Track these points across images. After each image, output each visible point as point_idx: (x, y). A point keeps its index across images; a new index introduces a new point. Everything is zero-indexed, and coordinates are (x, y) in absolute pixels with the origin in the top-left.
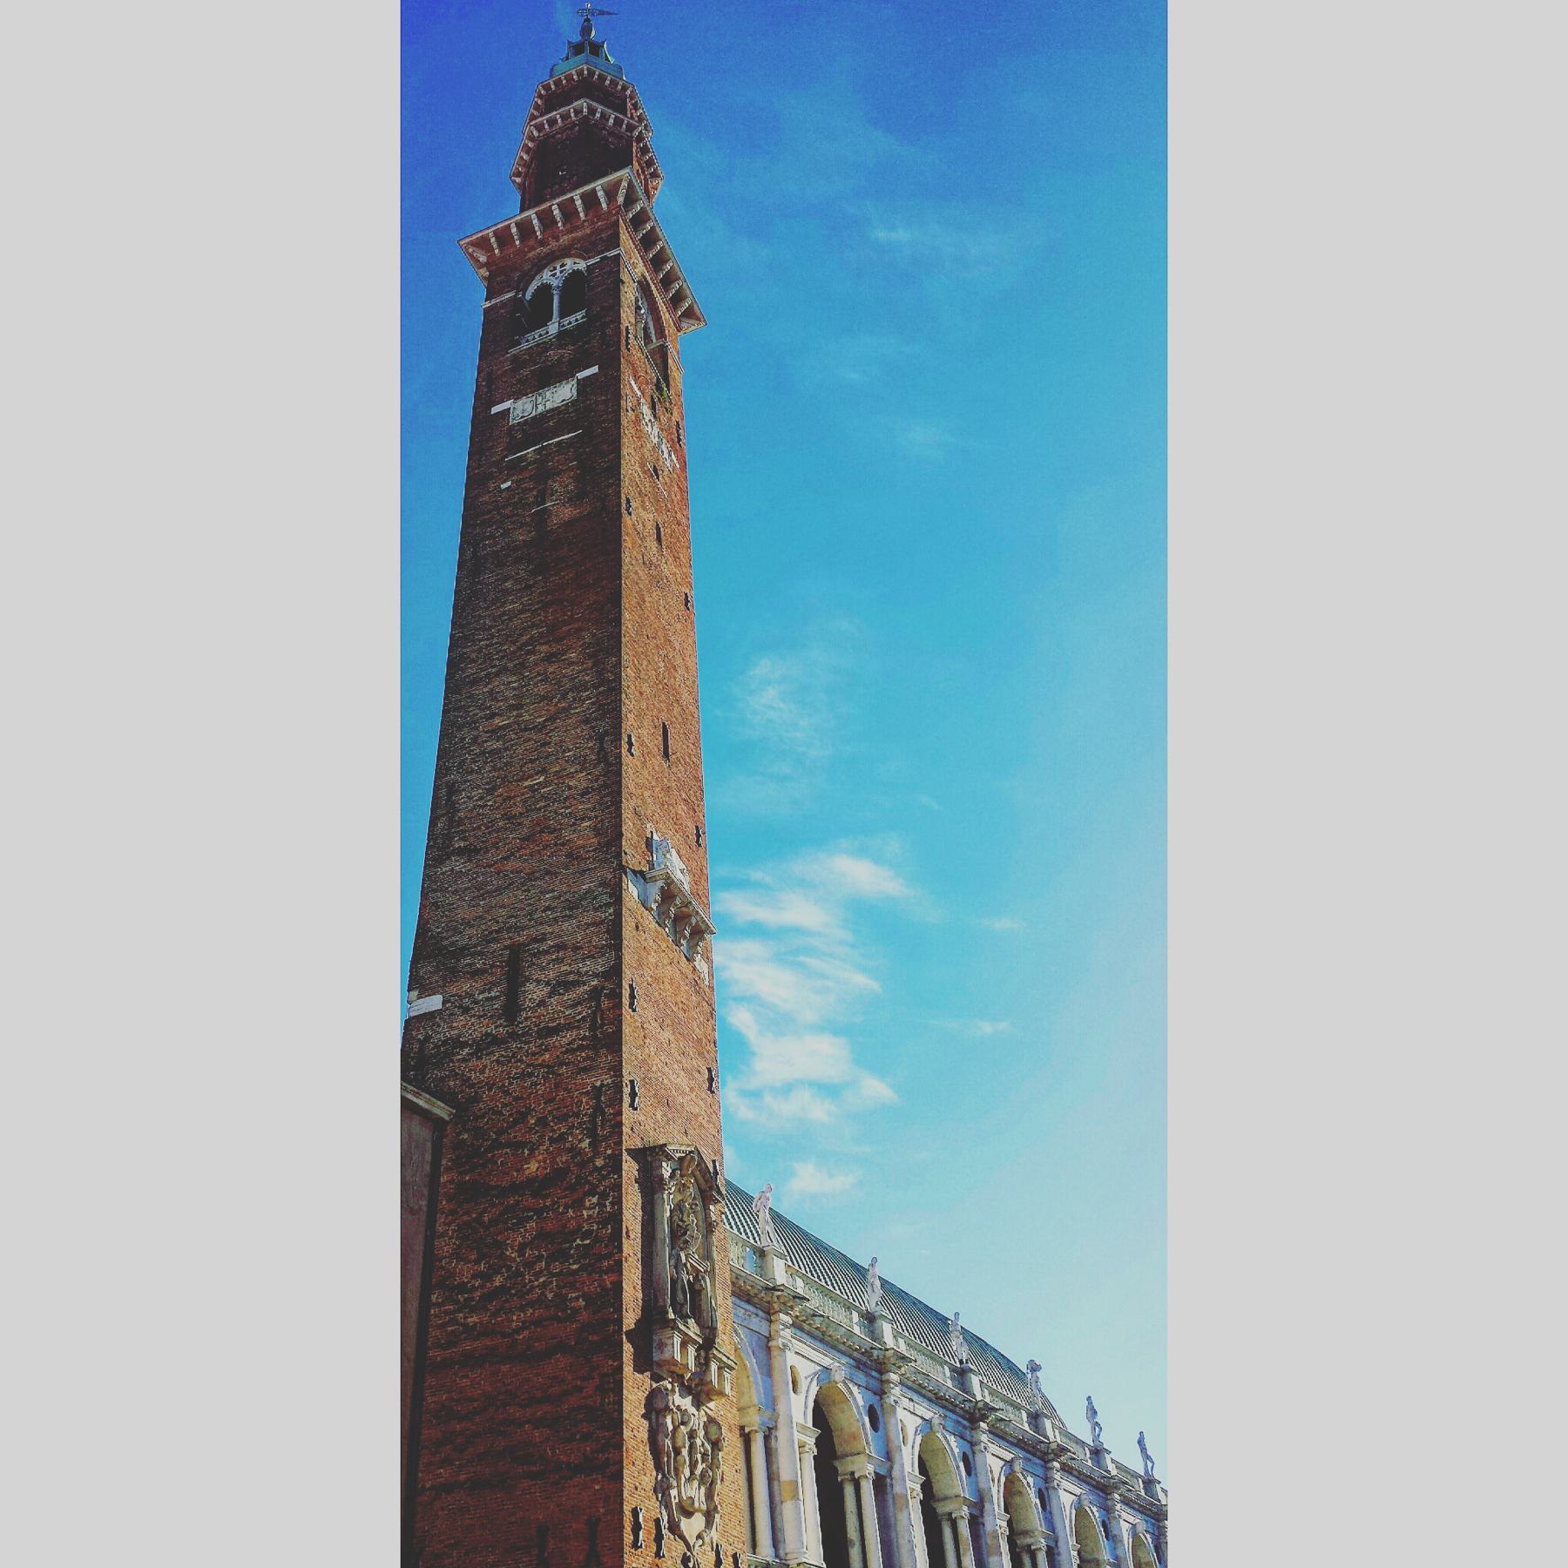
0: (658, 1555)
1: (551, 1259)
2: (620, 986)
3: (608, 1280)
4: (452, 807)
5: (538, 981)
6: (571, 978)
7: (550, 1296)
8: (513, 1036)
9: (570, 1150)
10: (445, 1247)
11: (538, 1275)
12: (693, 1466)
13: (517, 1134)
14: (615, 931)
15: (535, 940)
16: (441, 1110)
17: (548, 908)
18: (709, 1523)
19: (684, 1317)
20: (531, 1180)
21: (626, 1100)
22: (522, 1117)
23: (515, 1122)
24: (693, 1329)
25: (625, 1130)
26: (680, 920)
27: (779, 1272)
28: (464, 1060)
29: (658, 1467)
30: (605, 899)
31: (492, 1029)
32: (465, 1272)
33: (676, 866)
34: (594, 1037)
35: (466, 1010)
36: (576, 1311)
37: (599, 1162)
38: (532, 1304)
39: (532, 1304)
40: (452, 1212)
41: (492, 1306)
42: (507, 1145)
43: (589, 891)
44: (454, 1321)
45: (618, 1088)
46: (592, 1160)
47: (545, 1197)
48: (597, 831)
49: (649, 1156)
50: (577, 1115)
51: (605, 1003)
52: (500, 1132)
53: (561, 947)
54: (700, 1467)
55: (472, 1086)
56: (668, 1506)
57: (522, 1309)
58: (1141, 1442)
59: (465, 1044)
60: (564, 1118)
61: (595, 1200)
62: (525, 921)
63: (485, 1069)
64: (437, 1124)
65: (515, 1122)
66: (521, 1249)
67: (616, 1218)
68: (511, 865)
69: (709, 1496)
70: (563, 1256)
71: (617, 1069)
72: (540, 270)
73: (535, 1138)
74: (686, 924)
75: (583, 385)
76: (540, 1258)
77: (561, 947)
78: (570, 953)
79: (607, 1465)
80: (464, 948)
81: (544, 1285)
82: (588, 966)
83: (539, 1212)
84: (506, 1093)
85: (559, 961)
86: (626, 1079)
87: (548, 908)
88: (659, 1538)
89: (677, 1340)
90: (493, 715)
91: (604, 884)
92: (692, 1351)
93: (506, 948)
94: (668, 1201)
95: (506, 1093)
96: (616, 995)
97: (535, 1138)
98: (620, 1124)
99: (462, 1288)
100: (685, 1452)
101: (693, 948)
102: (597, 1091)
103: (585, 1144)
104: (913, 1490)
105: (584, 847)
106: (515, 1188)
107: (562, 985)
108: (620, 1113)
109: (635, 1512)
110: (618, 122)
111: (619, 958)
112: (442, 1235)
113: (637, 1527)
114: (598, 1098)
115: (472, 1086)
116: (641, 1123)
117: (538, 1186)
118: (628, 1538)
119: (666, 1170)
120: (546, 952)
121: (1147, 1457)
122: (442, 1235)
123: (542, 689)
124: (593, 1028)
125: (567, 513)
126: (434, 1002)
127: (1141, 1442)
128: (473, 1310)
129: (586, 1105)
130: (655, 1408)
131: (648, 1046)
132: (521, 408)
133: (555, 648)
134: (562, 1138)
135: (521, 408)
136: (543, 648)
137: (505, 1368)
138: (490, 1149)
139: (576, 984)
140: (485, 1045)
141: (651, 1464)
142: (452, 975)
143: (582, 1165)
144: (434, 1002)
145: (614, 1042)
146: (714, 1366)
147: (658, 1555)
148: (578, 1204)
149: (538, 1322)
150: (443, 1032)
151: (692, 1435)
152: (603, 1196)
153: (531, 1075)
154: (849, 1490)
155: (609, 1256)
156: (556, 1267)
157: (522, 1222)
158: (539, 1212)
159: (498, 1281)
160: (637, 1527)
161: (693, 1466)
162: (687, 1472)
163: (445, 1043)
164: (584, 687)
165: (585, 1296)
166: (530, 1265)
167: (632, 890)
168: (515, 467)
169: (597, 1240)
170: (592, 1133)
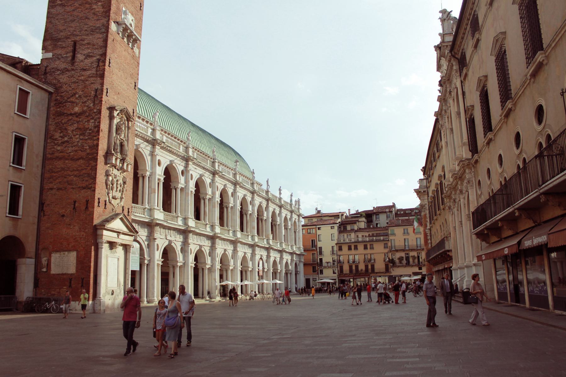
0: (105, 208)
1: (81, 135)
2: (105, 59)
3: (95, 142)
5: (81, 54)
6: (91, 54)
7: (80, 144)
8: (73, 70)
9: (87, 106)
10: (52, 128)
11: (77, 138)
12: (117, 188)
13: (72, 99)
14: (106, 41)
15: (81, 40)
16: (51, 90)
17: (86, 30)
18: (121, 201)
19: (117, 153)
20: (75, 114)
21: (105, 93)
22: (75, 94)
23: (72, 96)
24: (119, 156)
25: (103, 102)
26: (130, 36)
27: (158, 136)
28: (58, 75)
29: (107, 188)
30: (103, 30)
31: (67, 67)
32: (57, 135)
33: (129, 20)
34: (97, 74)
35: (59, 59)
36: (86, 149)
37: (95, 111)
38: (75, 146)
39: (75, 146)
40: (54, 119)
41: (64, 145)
42: (70, 102)
43: (99, 27)
44: (54, 148)
45: (102, 90)
46: (93, 110)
47: (80, 118)
48: (103, 7)
49: (111, 109)
50: (90, 96)
51: (101, 64)
52: (68, 98)
54: (119, 188)
55: (60, 83)
56: (109, 197)
57: (72, 147)
58: (267, 182)
59: (58, 70)
60: (86, 97)
61: (93, 121)
62: (79, 33)
63: (64, 78)
64: (50, 93)
65: (72, 96)
66: (73, 131)
67: (98, 127)
68: (75, 13)
69: (122, 195)
70: (83, 134)
71: (102, 84)
73: (78, 101)
74: (132, 38)
76: (77, 134)
77: (88, 44)
78: (91, 46)
79: (92, 188)
80: (60, 39)
81: (78, 142)
82: (96, 52)
83: (78, 122)
84: (70, 87)
85: (88, 48)
86: (105, 87)
87: (86, 30)
88: (106, 204)
89: (114, 158)
91: (103, 25)
92: (118, 160)
93: (72, 41)
94: (116, 121)
95: (70, 87)
96: (104, 62)
97: (78, 101)
98: (102, 101)
99: (56, 139)
100: (115, 185)
101: (133, 46)
102: (96, 90)
103: (92, 105)
104: (191, 192)
105: (99, 11)
106: (71, 114)
107: (88, 56)
108: (102, 98)
109: (99, 199)
111: (106, 50)
112: (51, 125)
113: (99, 202)
114: (96, 92)
115: (60, 83)
116: (108, 100)
117: (78, 115)
118: (96, 204)
119: (115, 113)
120: (84, 45)
121: (268, 185)
122: (51, 125)
124: (97, 71)
126: (50, 55)
127: (267, 182)
128: (59, 145)
129: (93, 93)
130: (107, 175)
131: (114, 77)
134: (85, 102)
138: (65, 102)
139: (92, 56)
141: (105, 187)
142: (55, 47)
143: (90, 110)
144: (50, 55)
145: (102, 76)
146: (125, 164)
147: (105, 208)
148: (88, 121)
149: (76, 151)
150: (53, 65)
151: (117, 181)
152: (95, 120)
153: (77, 82)
154: (174, 191)
155: (95, 136)
156: (81, 137)
157: (73, 124)
158: (78, 122)
159: (66, 139)
160: (99, 202)
161: (117, 188)
162: (115, 189)
163: (53, 68)
165: (89, 146)
166: (75, 136)
167: (113, 27)
169: (93, 132)
170: (94, 102)
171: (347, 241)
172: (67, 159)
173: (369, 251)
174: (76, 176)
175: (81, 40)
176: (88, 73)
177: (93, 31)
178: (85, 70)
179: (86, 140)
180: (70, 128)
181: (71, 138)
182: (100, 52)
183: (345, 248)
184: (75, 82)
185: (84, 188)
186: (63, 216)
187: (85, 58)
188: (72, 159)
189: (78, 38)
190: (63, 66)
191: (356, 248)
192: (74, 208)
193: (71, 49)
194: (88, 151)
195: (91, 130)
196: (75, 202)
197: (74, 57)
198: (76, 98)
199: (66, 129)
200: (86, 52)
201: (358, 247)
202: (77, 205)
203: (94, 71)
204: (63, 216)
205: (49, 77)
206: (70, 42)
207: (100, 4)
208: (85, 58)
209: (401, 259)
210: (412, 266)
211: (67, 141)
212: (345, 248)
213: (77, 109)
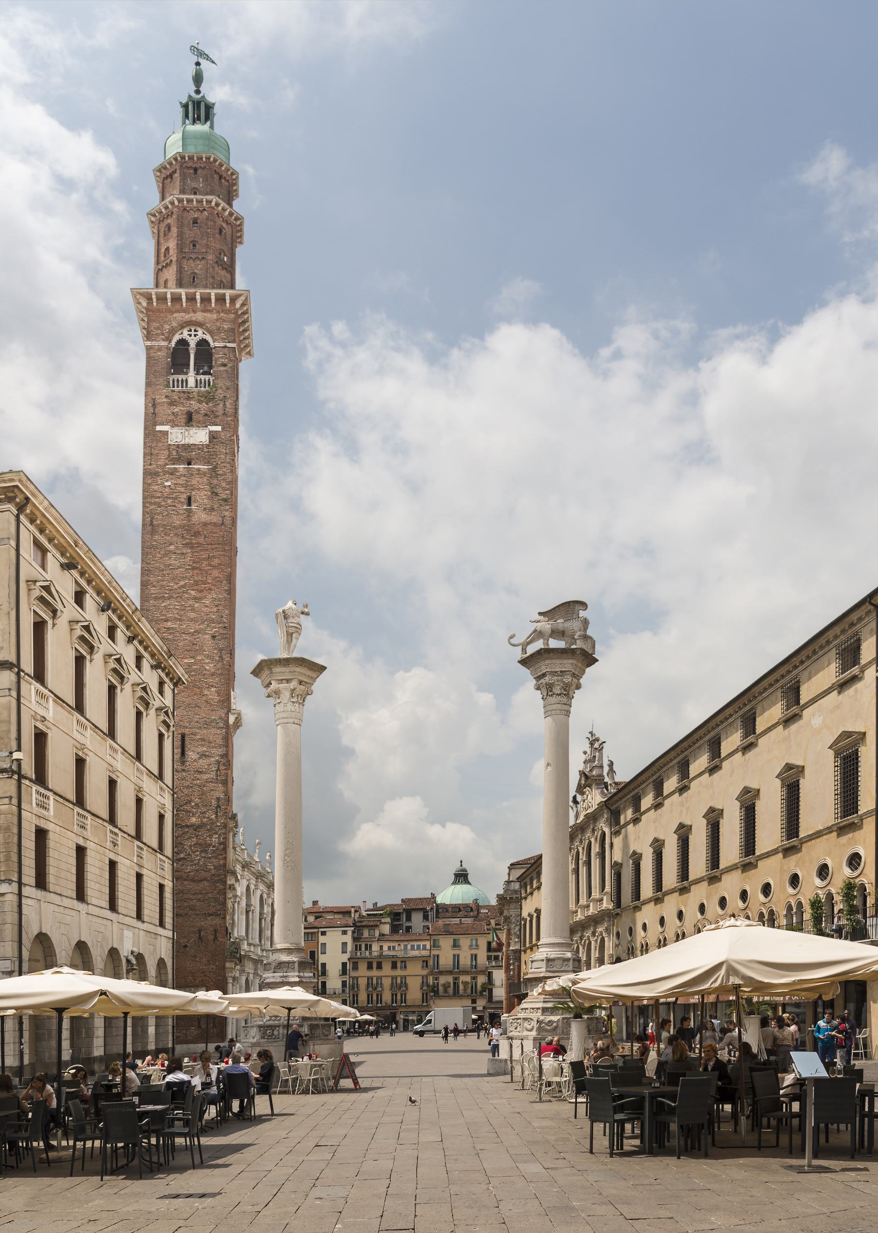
8: (184, 770)
11: (197, 856)
15: (192, 734)
20: (192, 826)
23: (186, 803)
36: (210, 869)
37: (219, 824)
41: (180, 863)
53: (203, 740)
62: (187, 725)
65: (186, 803)
66: (191, 846)
70: (206, 851)
72: (182, 327)
77: (203, 740)
82: (214, 751)
90: (166, 621)
103: (213, 816)
106: (187, 826)
107: (203, 755)
110: (224, 210)
117: (197, 828)
123: (192, 615)
132: (177, 436)
133: (199, 595)
134: (204, 813)
136: (193, 593)
137: (186, 883)
148: (211, 836)
149: (197, 871)
156: (203, 855)
157: (190, 838)
159: (182, 856)
164: (212, 621)
168: (172, 473)
170: (216, 813)
172: (185, 880)
173: (398, 972)
174: (199, 900)
175: (192, 734)
176: (205, 777)
177: (207, 724)
178: (201, 772)
179: (210, 858)
180: (187, 843)
181: (189, 854)
182: (220, 751)
183: (362, 966)
184: (188, 787)
185: (211, 915)
186: (185, 946)
187: (199, 758)
188: (192, 880)
189: (187, 731)
191: (379, 966)
192: (200, 938)
194: (213, 871)
195: (214, 846)
196: (200, 931)
198: (192, 807)
199: (182, 844)
201: (383, 965)
202: (202, 934)
203: (213, 775)
204: (185, 946)
207: (213, 689)
208: (199, 758)
209: (446, 986)
210: (461, 997)
211: (183, 859)
212: (362, 966)
213: (194, 820)
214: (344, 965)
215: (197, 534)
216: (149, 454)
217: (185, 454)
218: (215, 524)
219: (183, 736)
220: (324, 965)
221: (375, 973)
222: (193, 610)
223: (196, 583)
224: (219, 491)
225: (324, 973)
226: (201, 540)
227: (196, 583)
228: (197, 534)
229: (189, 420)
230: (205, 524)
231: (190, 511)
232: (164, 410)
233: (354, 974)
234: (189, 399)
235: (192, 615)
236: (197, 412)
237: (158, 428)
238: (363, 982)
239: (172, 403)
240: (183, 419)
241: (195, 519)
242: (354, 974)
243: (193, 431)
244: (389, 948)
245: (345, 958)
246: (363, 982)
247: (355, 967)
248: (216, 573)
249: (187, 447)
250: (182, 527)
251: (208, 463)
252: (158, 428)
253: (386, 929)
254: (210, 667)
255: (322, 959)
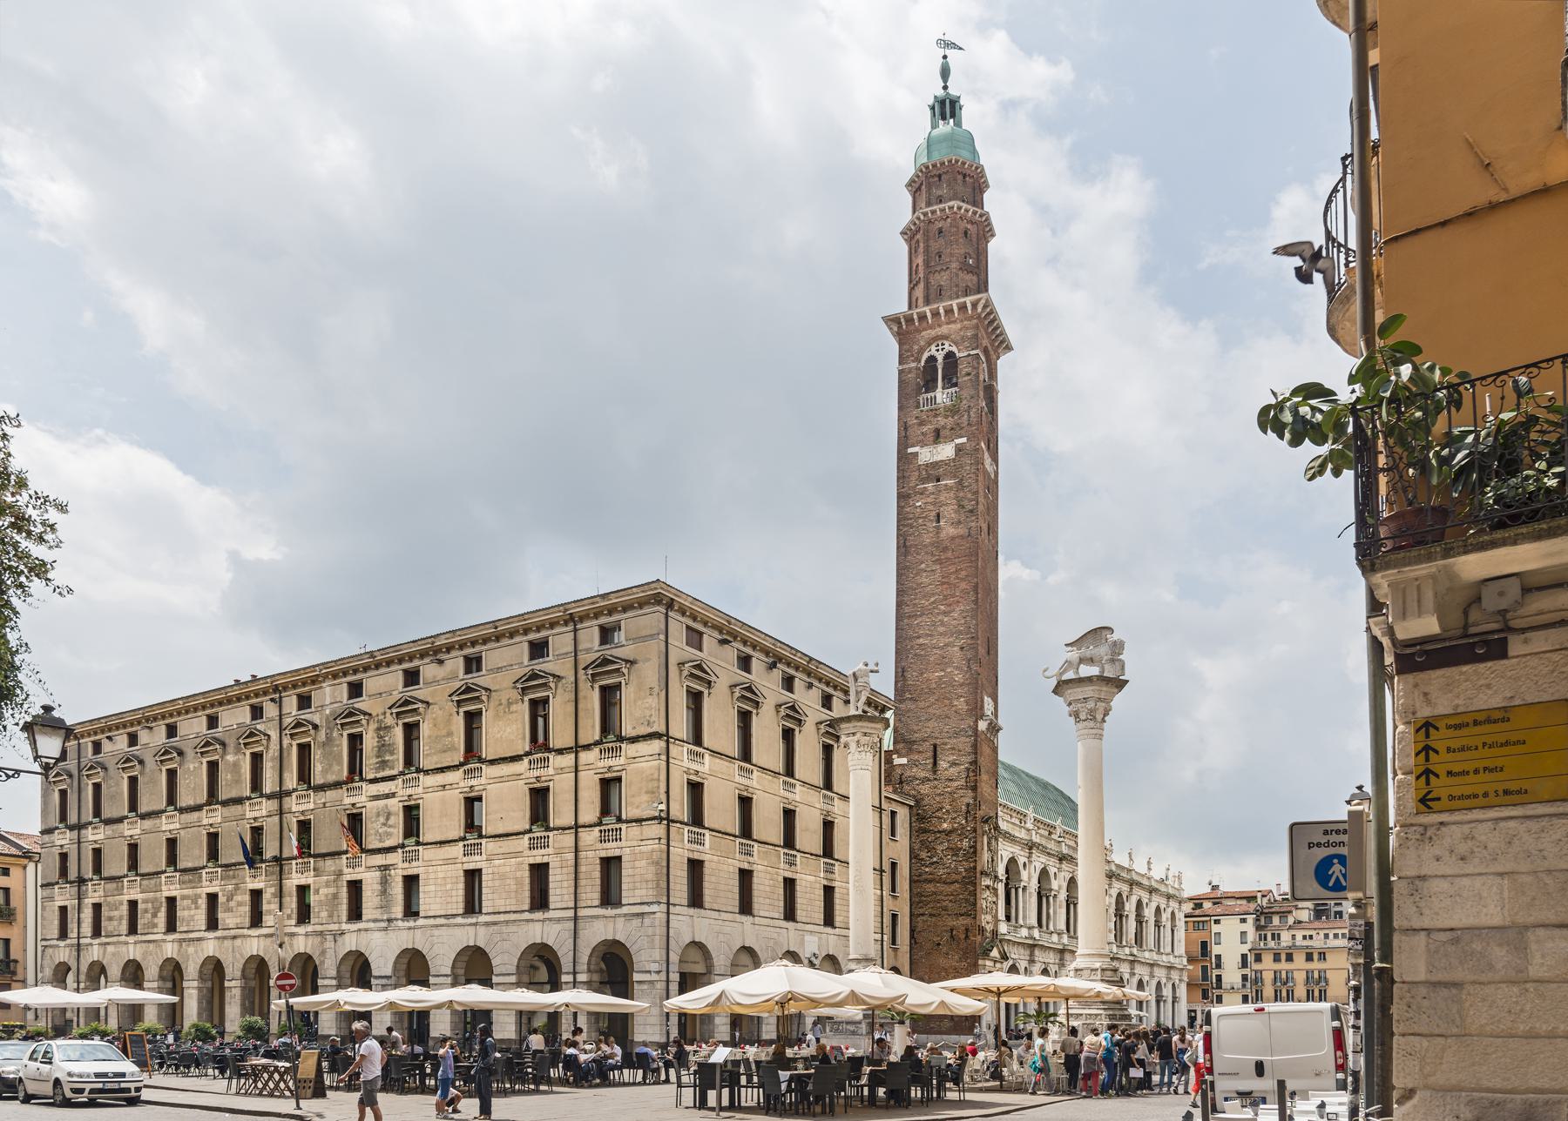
4: (905, 679)
63: (925, 789)
75: (959, 449)
107: (953, 764)
123: (941, 629)
125: (952, 531)
132: (926, 455)
135: (926, 455)
140: (925, 780)
150: (908, 773)
164: (960, 632)
171: (1272, 944)
177: (957, 734)
182: (970, 758)
183: (1268, 959)
190: (923, 775)
191: (1290, 958)
193: (930, 754)
197: (935, 763)
200: (952, 758)
203: (963, 782)
205: (906, 788)
206: (927, 746)
212: (1268, 959)
214: (1244, 957)
215: (945, 549)
216: (902, 477)
217: (934, 472)
218: (962, 537)
219: (935, 746)
220: (1218, 957)
221: (1284, 966)
222: (943, 624)
223: (946, 598)
224: (965, 503)
225: (1219, 966)
226: (949, 554)
227: (946, 598)
228: (945, 549)
229: (937, 437)
230: (953, 538)
231: (938, 528)
232: (915, 432)
233: (1257, 967)
234: (936, 416)
235: (941, 629)
236: (944, 427)
237: (910, 450)
238: (1268, 977)
239: (922, 423)
240: (931, 438)
241: (943, 535)
242: (1257, 967)
243: (940, 447)
244: (1304, 937)
245: (1245, 949)
246: (1268, 977)
247: (1258, 959)
248: (963, 585)
249: (935, 465)
250: (932, 544)
251: (955, 477)
252: (910, 450)
253: (1304, 915)
254: (959, 678)
255: (1216, 950)
